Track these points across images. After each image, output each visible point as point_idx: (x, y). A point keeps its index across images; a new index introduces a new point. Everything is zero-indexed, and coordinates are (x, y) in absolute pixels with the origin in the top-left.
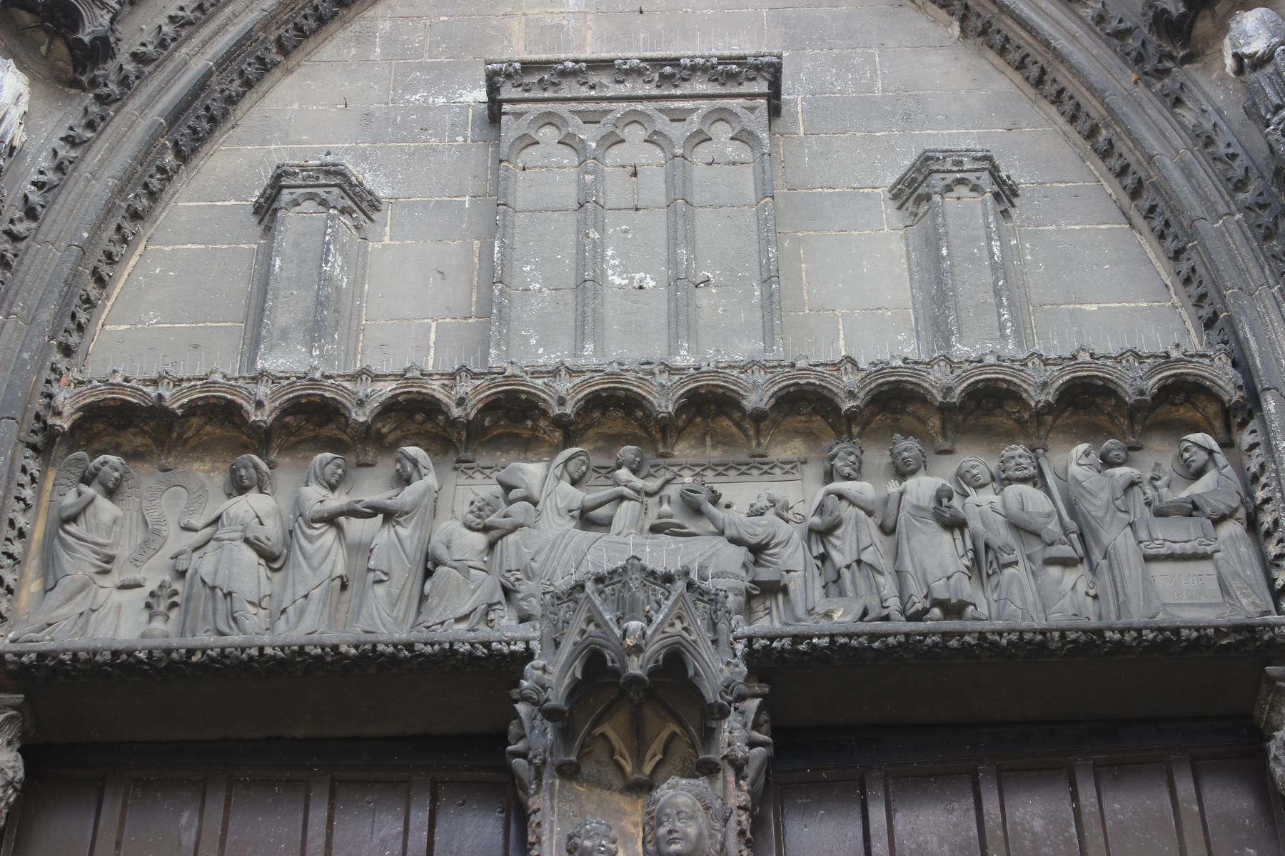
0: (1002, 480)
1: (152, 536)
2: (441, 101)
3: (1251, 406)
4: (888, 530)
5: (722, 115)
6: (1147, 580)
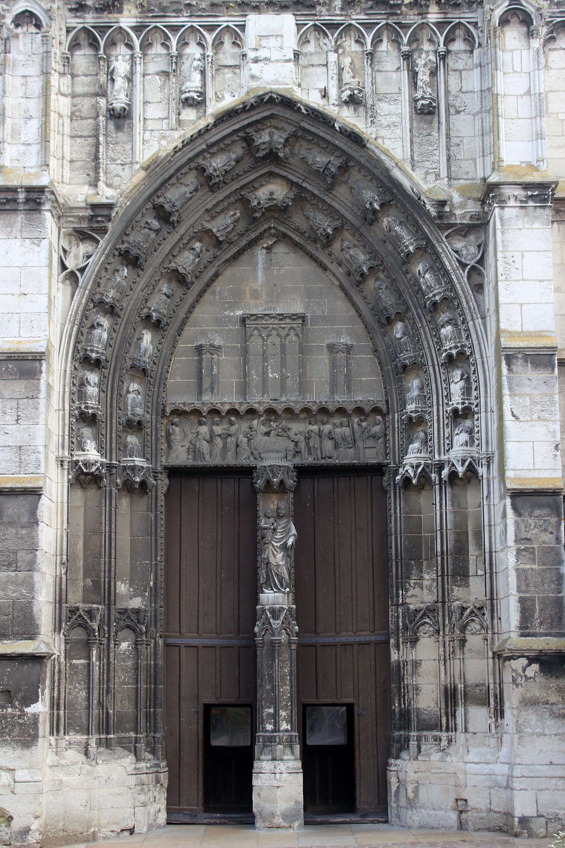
0: (341, 425)
1: (185, 435)
2: (232, 314)
3: (388, 413)
4: (320, 436)
5: (292, 328)
6: (364, 453)
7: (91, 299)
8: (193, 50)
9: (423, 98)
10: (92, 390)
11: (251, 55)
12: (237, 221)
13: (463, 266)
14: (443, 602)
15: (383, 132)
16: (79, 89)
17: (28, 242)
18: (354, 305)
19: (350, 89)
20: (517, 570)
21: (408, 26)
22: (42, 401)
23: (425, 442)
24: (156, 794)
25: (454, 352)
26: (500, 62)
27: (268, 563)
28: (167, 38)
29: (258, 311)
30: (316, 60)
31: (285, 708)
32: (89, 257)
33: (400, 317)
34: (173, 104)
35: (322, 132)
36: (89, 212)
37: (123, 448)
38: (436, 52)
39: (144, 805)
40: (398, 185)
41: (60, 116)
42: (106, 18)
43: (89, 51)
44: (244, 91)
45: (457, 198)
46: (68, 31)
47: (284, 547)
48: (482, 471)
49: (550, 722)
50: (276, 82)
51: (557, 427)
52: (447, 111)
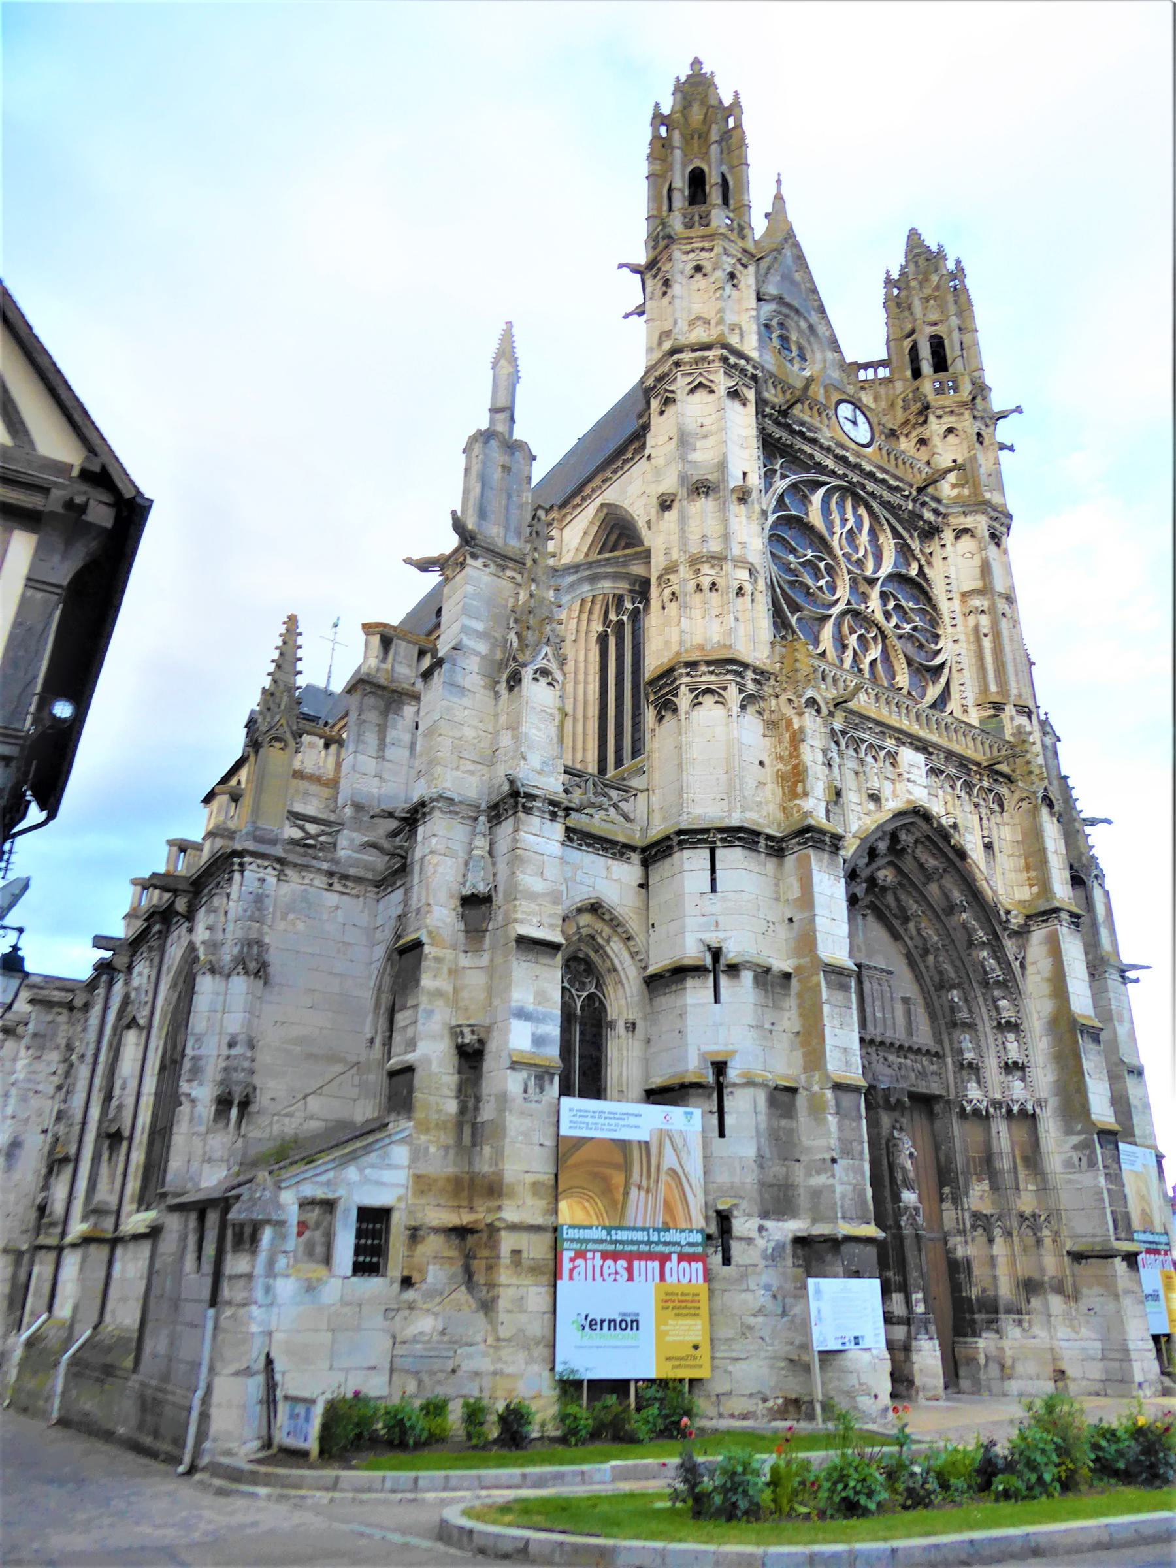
11: (906, 776)
23: (979, 1082)
33: (958, 986)
35: (942, 844)
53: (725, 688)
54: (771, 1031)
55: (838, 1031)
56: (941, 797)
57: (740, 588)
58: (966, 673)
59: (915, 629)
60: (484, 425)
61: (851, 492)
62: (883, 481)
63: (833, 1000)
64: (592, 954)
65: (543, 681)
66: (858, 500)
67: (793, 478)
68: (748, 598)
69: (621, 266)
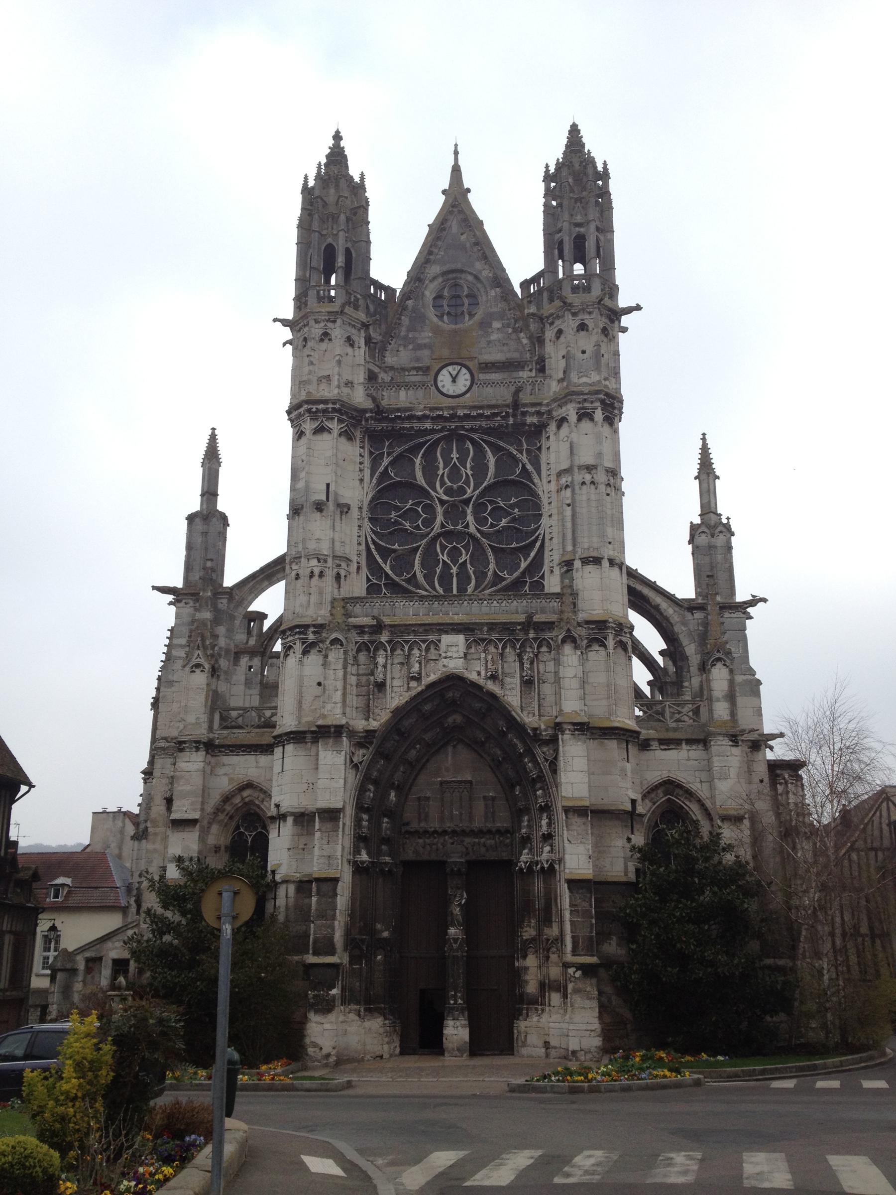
0: (490, 839)
7: (364, 776)
8: (416, 652)
9: (526, 676)
10: (365, 823)
11: (443, 655)
12: (438, 733)
13: (547, 760)
14: (539, 936)
15: (507, 693)
16: (361, 672)
17: (335, 752)
18: (497, 776)
19: (492, 672)
20: (570, 921)
21: (519, 640)
22: (340, 833)
23: (530, 850)
24: (394, 1038)
25: (543, 804)
26: (561, 661)
27: (452, 914)
28: (404, 646)
29: (448, 779)
30: (475, 657)
31: (460, 992)
32: (364, 756)
34: (406, 679)
36: (365, 734)
37: (380, 853)
38: (533, 652)
39: (388, 1043)
40: (515, 719)
41: (352, 686)
42: (374, 637)
43: (365, 653)
44: (440, 672)
45: (543, 727)
46: (356, 643)
47: (460, 905)
48: (557, 867)
49: (587, 1002)
50: (455, 668)
51: (590, 847)
52: (538, 682)
53: (295, 644)
54: (303, 849)
55: (325, 847)
56: (482, 659)
57: (312, 572)
58: (555, 541)
59: (514, 520)
60: (197, 508)
61: (455, 437)
62: (480, 416)
63: (323, 829)
64: (257, 810)
65: (198, 671)
66: (461, 439)
67: (398, 450)
68: (316, 577)
69: (284, 345)
